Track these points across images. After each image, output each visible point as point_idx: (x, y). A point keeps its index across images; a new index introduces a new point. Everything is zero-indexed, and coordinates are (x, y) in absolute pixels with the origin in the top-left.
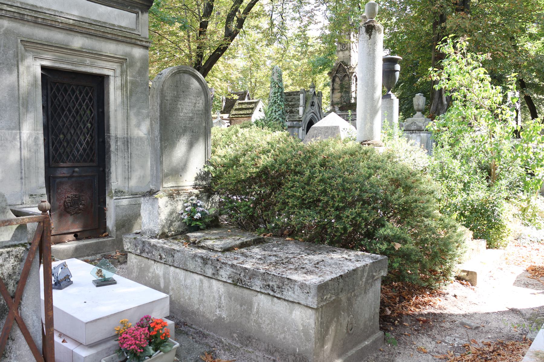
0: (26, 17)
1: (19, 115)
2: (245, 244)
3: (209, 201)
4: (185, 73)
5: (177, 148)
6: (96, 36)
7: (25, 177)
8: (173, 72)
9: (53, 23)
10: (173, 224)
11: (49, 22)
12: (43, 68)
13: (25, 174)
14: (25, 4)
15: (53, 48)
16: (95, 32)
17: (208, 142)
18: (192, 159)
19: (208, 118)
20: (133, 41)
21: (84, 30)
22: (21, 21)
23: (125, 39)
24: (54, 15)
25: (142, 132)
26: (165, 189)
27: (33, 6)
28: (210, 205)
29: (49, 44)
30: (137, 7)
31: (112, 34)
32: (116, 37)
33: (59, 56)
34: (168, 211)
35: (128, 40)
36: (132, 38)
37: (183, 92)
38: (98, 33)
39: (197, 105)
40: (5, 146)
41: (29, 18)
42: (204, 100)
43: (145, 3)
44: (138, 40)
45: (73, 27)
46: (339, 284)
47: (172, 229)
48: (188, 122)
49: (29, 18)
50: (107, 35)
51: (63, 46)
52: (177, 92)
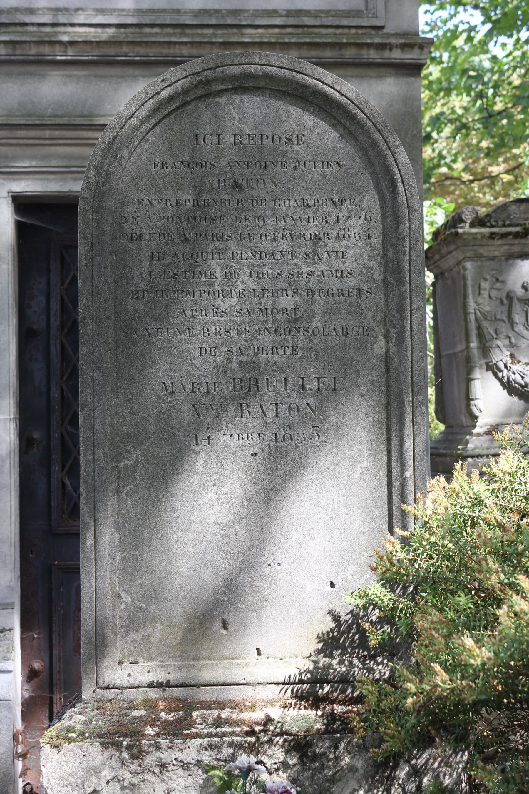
3: (391, 779)
8: (165, 93)
9: (46, 50)
11: (33, 51)
15: (48, 133)
17: (401, 444)
18: (295, 535)
19: (401, 309)
20: (350, 53)
21: (152, 51)
26: (111, 694)
33: (70, 157)
36: (341, 46)
37: (236, 185)
42: (376, 214)
44: (369, 46)
45: (112, 51)
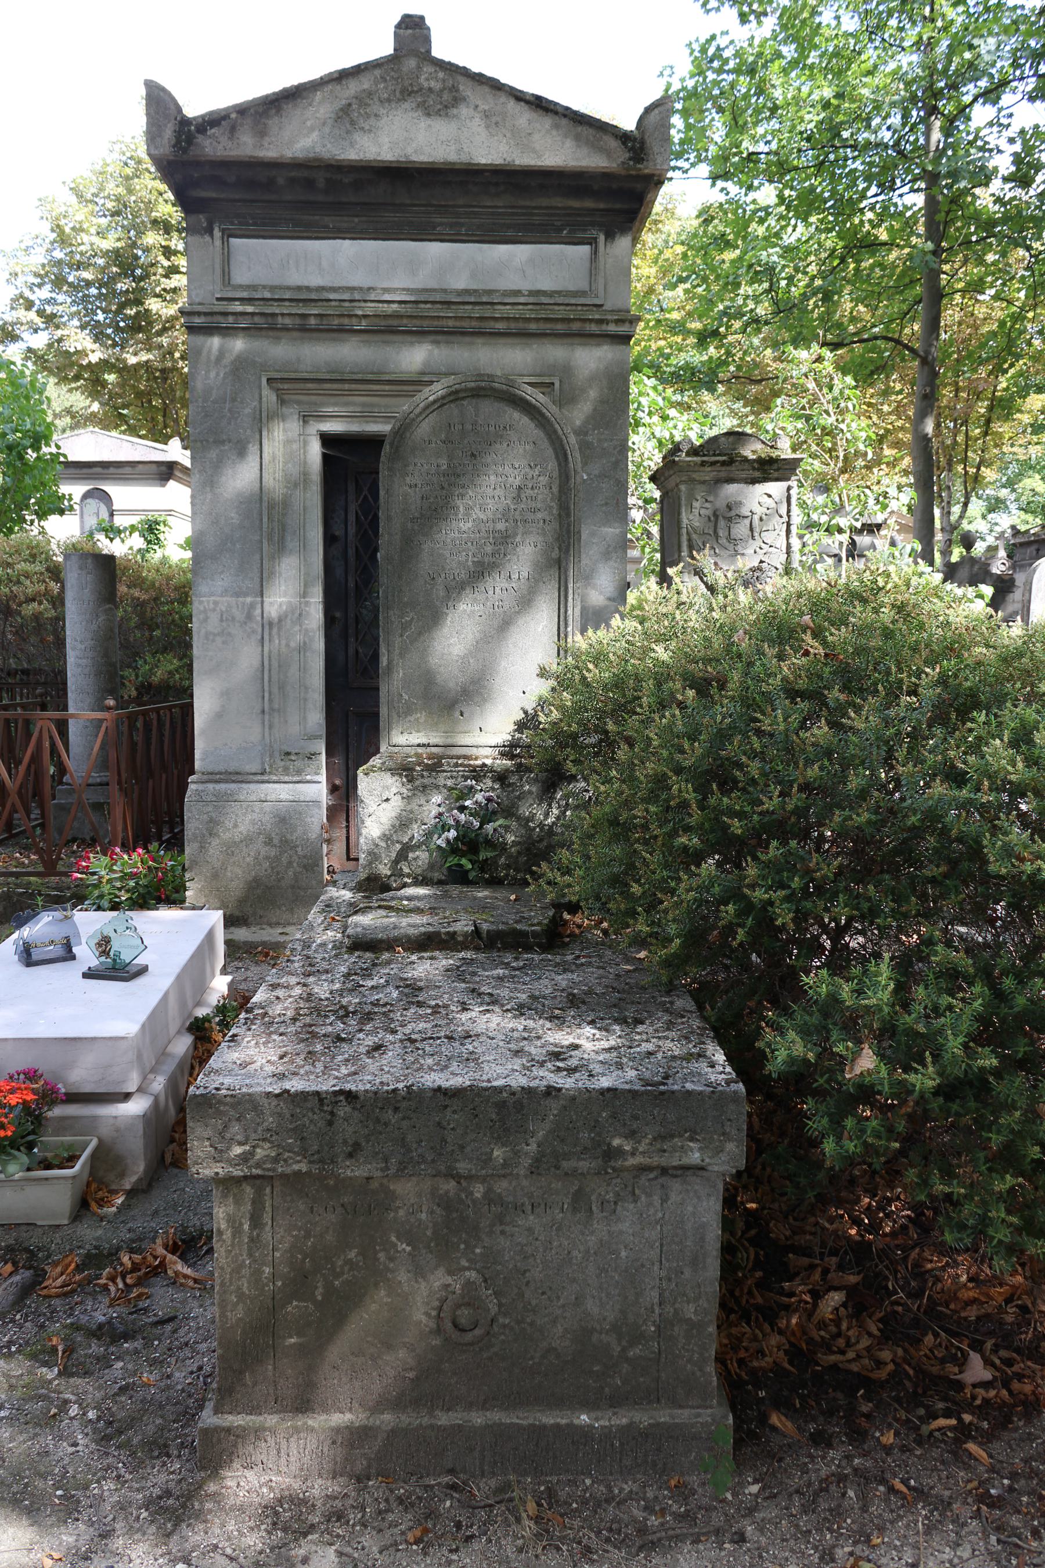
0: (280, 319)
1: (262, 560)
2: (445, 941)
3: (552, 798)
4: (478, 396)
5: (445, 631)
6: (463, 334)
7: (272, 709)
8: (431, 398)
9: (346, 321)
10: (411, 855)
11: (336, 322)
12: (327, 440)
13: (271, 700)
14: (281, 288)
15: (347, 386)
16: (458, 324)
17: (566, 612)
18: (503, 664)
19: (568, 532)
20: (576, 326)
21: (426, 323)
22: (271, 333)
23: (549, 326)
24: (351, 301)
25: (601, 593)
26: (396, 749)
27: (299, 288)
28: (555, 811)
29: (334, 376)
30: (593, 224)
31: (508, 319)
32: (521, 325)
33: (364, 405)
34: (394, 814)
35: (560, 327)
36: (569, 320)
37: (473, 455)
38: (465, 324)
39: (529, 492)
40: (229, 634)
41: (287, 321)
42: (556, 474)
43: (618, 206)
44: (591, 321)
45: (395, 322)
46: (330, 1123)
47: (406, 870)
48: (489, 549)
49: (287, 321)
50: (492, 324)
51: (370, 377)
52: (450, 458)
